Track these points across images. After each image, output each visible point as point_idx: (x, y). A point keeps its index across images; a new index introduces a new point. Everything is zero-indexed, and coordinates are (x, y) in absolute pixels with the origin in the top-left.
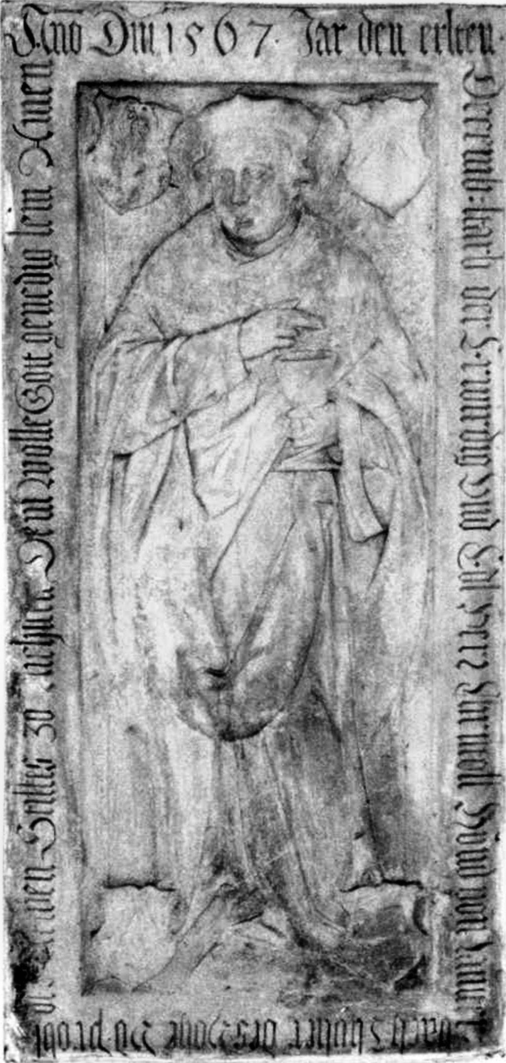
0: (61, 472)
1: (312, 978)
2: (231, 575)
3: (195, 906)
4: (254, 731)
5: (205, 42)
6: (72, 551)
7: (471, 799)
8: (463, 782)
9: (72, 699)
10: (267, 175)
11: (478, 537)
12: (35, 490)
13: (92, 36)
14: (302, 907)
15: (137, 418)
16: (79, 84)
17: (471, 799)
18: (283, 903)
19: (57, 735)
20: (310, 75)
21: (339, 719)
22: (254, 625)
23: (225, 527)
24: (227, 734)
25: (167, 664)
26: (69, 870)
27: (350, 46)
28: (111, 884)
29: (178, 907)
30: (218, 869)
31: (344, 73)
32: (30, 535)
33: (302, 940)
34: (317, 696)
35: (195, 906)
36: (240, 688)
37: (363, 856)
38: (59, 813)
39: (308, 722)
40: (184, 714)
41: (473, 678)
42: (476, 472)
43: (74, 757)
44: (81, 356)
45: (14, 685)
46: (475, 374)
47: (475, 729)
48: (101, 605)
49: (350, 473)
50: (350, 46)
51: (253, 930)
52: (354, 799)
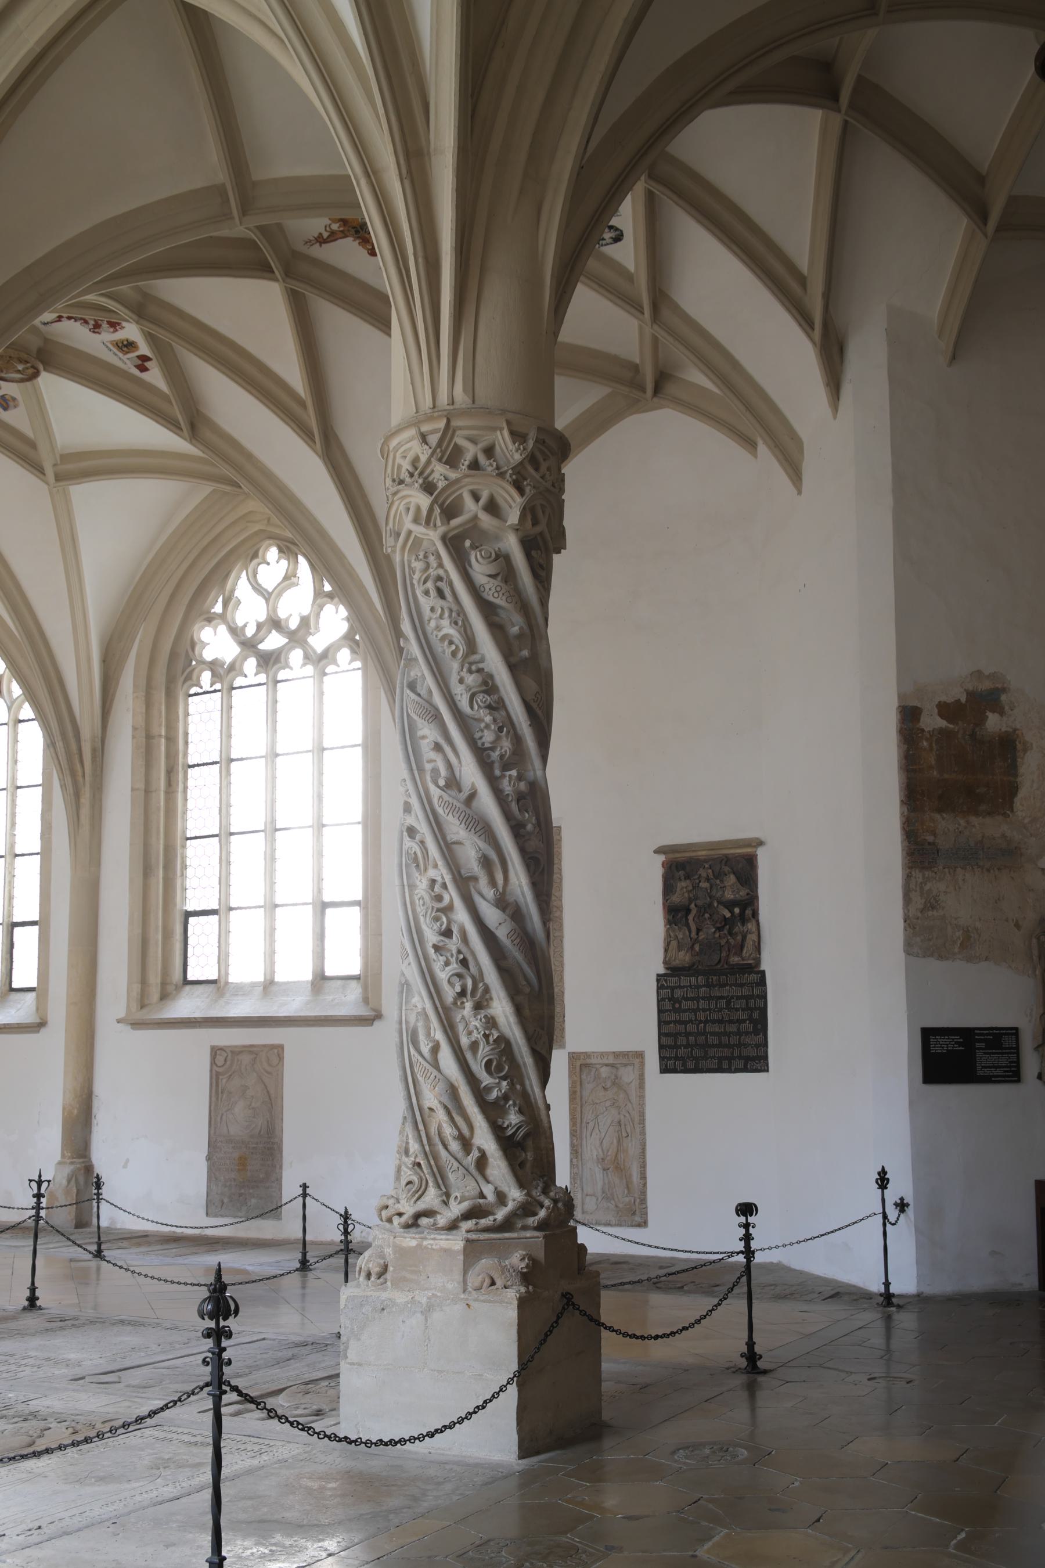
0: (578, 1125)
1: (618, 1213)
2: (604, 1142)
3: (600, 1200)
4: (608, 1169)
5: (599, 1058)
6: (581, 1139)
7: (642, 1182)
8: (641, 1179)
9: (580, 1163)
10: (609, 1077)
11: (643, 1137)
12: (574, 1128)
13: (582, 1057)
14: (616, 1200)
15: (589, 1117)
16: (581, 1065)
17: (642, 1182)
18: (614, 1199)
19: (578, 1168)
20: (615, 1062)
21: (622, 1167)
22: (608, 1151)
23: (603, 1134)
24: (604, 1170)
25: (595, 1157)
26: (580, 1191)
27: (621, 1058)
28: (587, 1195)
29: (597, 1200)
30: (603, 1192)
31: (620, 1062)
32: (574, 1135)
33: (616, 1206)
34: (618, 1163)
35: (600, 1200)
36: (606, 1162)
37: (626, 1192)
38: (578, 1182)
39: (616, 1168)
40: (598, 1166)
41: (641, 1160)
42: (642, 1126)
43: (580, 1173)
44: (581, 1107)
45: (571, 1161)
46: (641, 1110)
47: (642, 1169)
48: (585, 1147)
49: (623, 1126)
50: (621, 1058)
51: (609, 1204)
52: (625, 1181)
